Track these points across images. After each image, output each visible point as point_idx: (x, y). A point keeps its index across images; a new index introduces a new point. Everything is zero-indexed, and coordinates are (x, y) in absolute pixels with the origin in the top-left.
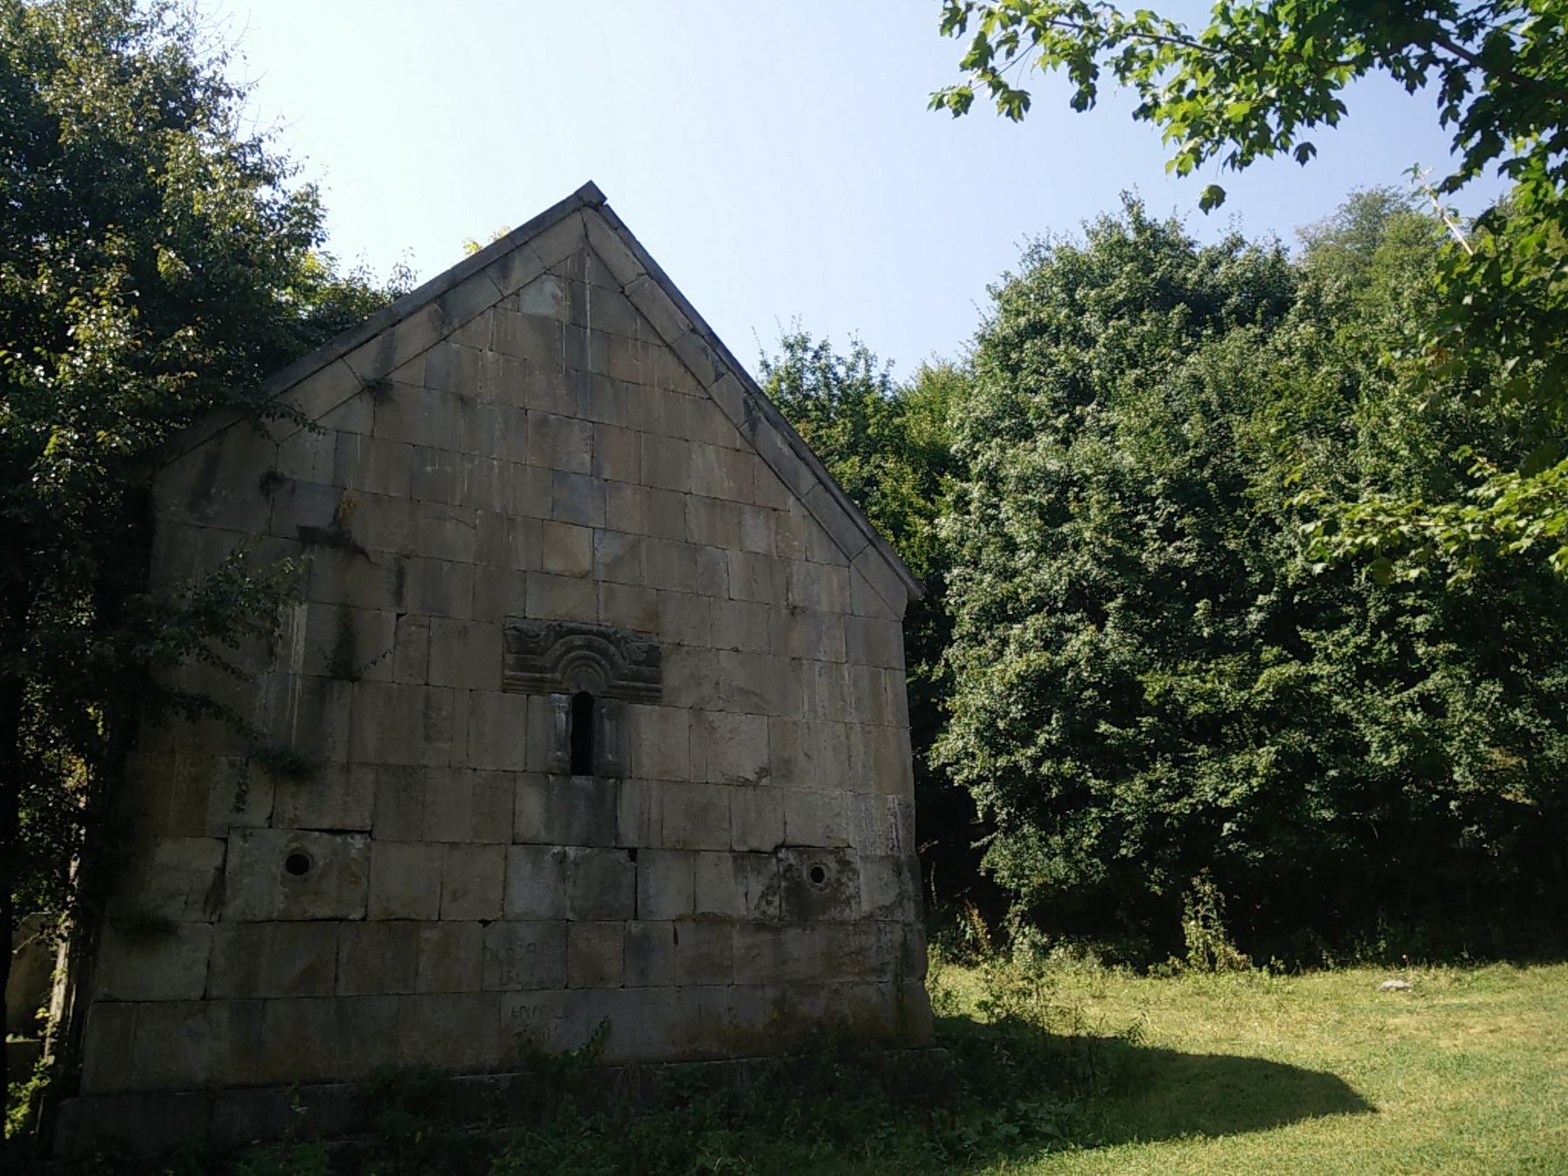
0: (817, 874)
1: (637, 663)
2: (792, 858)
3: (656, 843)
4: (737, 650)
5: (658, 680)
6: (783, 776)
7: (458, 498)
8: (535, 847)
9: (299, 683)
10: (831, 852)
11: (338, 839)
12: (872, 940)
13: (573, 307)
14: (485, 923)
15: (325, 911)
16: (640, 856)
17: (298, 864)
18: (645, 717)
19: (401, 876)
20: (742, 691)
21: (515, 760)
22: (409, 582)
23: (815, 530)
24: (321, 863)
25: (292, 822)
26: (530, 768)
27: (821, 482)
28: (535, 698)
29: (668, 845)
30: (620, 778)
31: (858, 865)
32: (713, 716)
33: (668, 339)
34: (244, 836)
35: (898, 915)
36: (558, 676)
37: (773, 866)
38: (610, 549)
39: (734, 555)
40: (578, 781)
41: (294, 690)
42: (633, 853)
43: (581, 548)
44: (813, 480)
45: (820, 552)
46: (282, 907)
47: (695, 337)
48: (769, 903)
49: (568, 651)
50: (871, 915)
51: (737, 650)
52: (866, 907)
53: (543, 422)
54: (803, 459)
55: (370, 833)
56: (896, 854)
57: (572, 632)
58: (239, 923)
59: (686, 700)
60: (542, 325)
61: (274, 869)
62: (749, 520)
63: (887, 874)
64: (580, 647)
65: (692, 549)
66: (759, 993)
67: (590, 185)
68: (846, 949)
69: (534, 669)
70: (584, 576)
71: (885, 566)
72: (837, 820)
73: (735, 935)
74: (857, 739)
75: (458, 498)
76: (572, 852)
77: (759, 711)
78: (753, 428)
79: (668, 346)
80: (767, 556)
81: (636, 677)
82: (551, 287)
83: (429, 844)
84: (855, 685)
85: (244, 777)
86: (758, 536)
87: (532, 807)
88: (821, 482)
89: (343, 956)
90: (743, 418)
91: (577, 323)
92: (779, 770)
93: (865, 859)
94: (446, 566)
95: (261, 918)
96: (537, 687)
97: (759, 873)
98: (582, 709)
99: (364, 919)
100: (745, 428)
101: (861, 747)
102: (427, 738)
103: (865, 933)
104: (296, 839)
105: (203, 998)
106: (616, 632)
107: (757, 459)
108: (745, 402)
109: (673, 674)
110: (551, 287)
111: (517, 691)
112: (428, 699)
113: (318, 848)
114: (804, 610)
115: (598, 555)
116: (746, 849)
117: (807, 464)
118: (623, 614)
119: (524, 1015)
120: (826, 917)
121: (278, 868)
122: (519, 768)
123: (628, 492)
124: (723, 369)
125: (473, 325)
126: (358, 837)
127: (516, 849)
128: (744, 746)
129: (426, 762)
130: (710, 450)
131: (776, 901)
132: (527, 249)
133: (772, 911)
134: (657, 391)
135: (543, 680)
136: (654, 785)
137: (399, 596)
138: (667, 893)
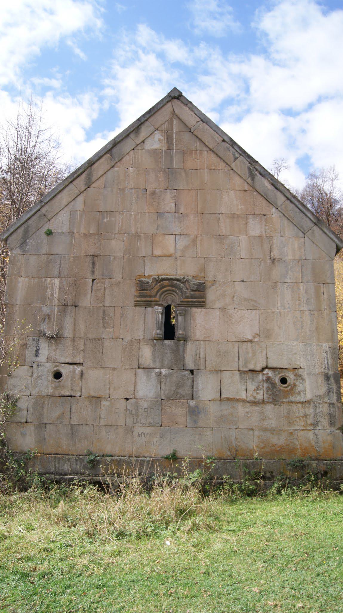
0: (284, 381)
1: (193, 290)
2: (270, 373)
3: (202, 368)
4: (243, 281)
5: (204, 297)
6: (266, 337)
7: (117, 229)
8: (147, 369)
9: (56, 309)
10: (291, 371)
11: (71, 367)
12: (311, 410)
13: (168, 142)
14: (127, 399)
15: (67, 393)
16: (194, 373)
17: (58, 375)
18: (198, 313)
19: (95, 380)
20: (246, 299)
21: (140, 335)
22: (97, 267)
23: (286, 222)
26: (146, 337)
27: (288, 199)
28: (149, 309)
29: (208, 369)
30: (185, 340)
31: (305, 376)
32: (231, 312)
33: (211, 148)
35: (326, 399)
36: (157, 298)
37: (260, 377)
38: (182, 243)
39: (243, 238)
40: (167, 342)
41: (54, 311)
42: (192, 372)
43: (169, 244)
44: (284, 199)
45: (289, 231)
46: (52, 391)
47: (224, 143)
48: (257, 393)
49: (161, 288)
50: (311, 400)
51: (243, 281)
52: (309, 396)
53: (154, 193)
54: (278, 190)
55: (82, 364)
56: (326, 371)
57: (163, 280)
59: (218, 305)
60: (154, 153)
62: (251, 222)
63: (321, 380)
64: (169, 286)
65: (221, 238)
66: (251, 432)
67: (175, 89)
68: (297, 415)
69: (146, 296)
70: (170, 256)
71: (323, 235)
72: (295, 356)
73: (239, 407)
74: (307, 318)
75: (117, 229)
76: (164, 371)
77: (255, 308)
78: (253, 179)
79: (211, 150)
80: (260, 237)
81: (192, 297)
82: (158, 136)
83: (104, 368)
84: (306, 292)
85: (38, 344)
86: (255, 228)
87: (147, 353)
88: (288, 199)
89: (73, 410)
90: (248, 175)
91: (170, 149)
92: (266, 334)
93: (309, 374)
94: (112, 258)
95: (44, 395)
96: (148, 304)
97: (253, 380)
98: (167, 311)
99: (80, 396)
100: (249, 180)
101: (309, 322)
102: (104, 327)
103: (308, 407)
104: (56, 366)
105: (26, 422)
106: (184, 278)
107: (255, 193)
108: (249, 169)
109: (211, 295)
110: (158, 136)
111: (141, 306)
112: (104, 311)
113: (65, 370)
114: (280, 260)
115: (177, 246)
116: (247, 369)
117: (281, 192)
118: (188, 270)
119: (143, 436)
120: (287, 400)
121: (51, 377)
122: (142, 337)
123: (192, 217)
124: (237, 155)
125: (124, 159)
127: (140, 370)
128: (247, 325)
129: (103, 336)
130: (232, 193)
131: (261, 392)
132: (147, 123)
133: (260, 397)
134: (206, 171)
135: (151, 301)
136: (202, 343)
137: (93, 272)
138: (206, 388)
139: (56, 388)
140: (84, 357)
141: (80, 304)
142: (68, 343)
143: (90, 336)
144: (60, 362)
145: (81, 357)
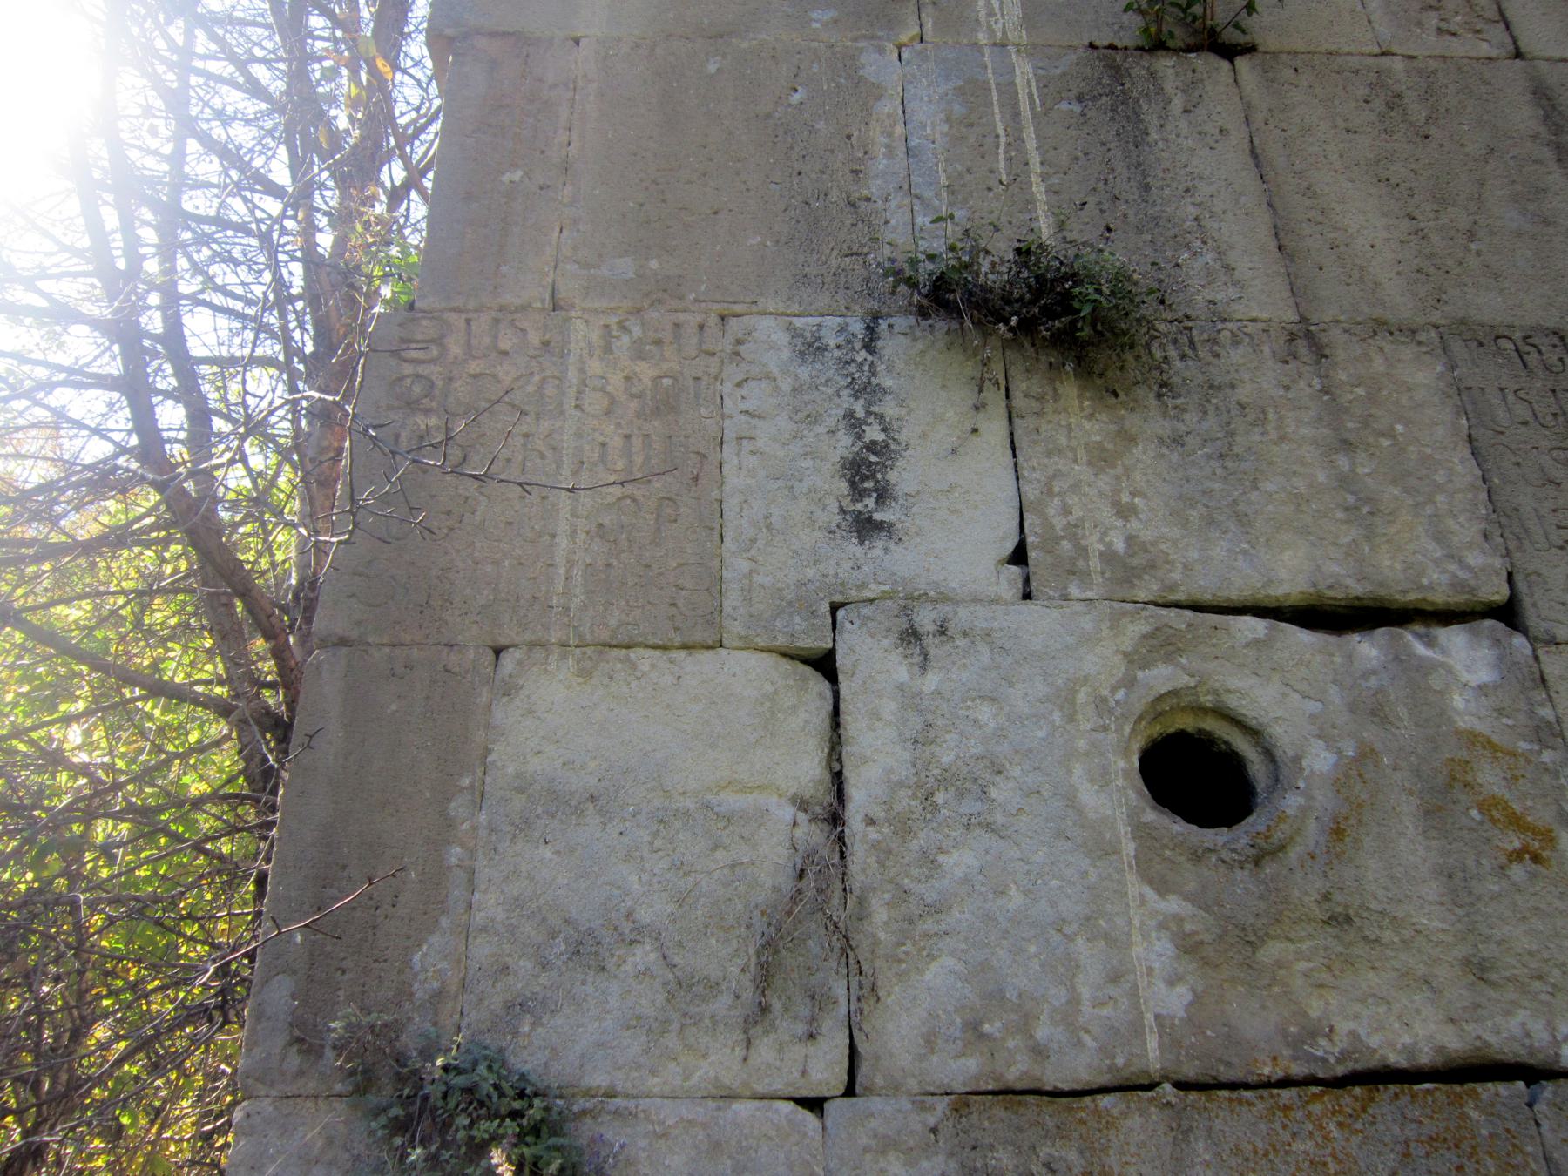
9: (1023, 71)
11: (1368, 648)
15: (1416, 1030)
24: (1320, 760)
25: (1125, 568)
34: (911, 636)
41: (1009, 92)
46: (1175, 1001)
58: (963, 1101)
61: (1088, 796)
85: (866, 390)
104: (1161, 646)
113: (1283, 693)
121: (1113, 794)
126: (1454, 638)
139: (1225, 948)
140: (1501, 520)
141: (1268, 41)
142: (1255, 373)
143: (1489, 306)
144: (1205, 587)
145: (1465, 530)
